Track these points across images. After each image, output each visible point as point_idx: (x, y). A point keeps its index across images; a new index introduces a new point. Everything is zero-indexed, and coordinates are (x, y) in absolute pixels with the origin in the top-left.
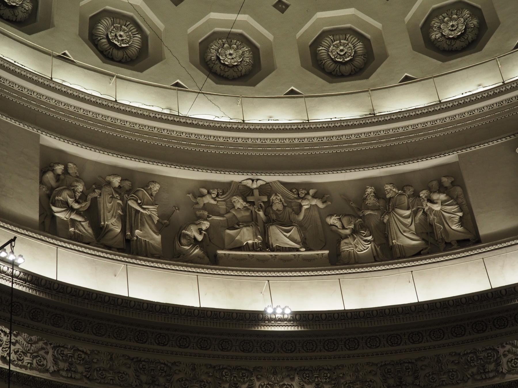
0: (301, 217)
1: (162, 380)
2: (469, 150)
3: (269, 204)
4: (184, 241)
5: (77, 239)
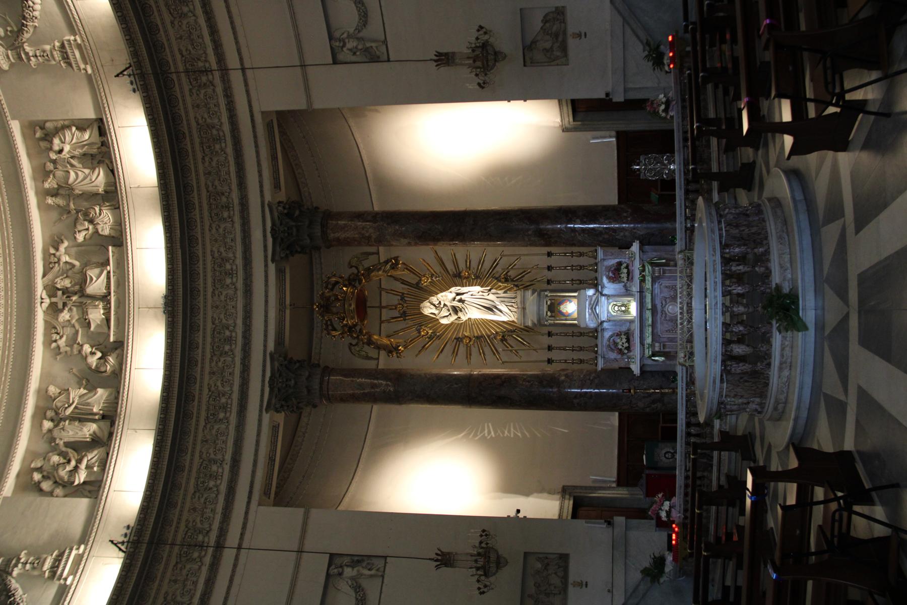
0: (77, 263)
1: (223, 400)
2: (6, 110)
3: (65, 291)
4: (103, 369)
5: (104, 464)
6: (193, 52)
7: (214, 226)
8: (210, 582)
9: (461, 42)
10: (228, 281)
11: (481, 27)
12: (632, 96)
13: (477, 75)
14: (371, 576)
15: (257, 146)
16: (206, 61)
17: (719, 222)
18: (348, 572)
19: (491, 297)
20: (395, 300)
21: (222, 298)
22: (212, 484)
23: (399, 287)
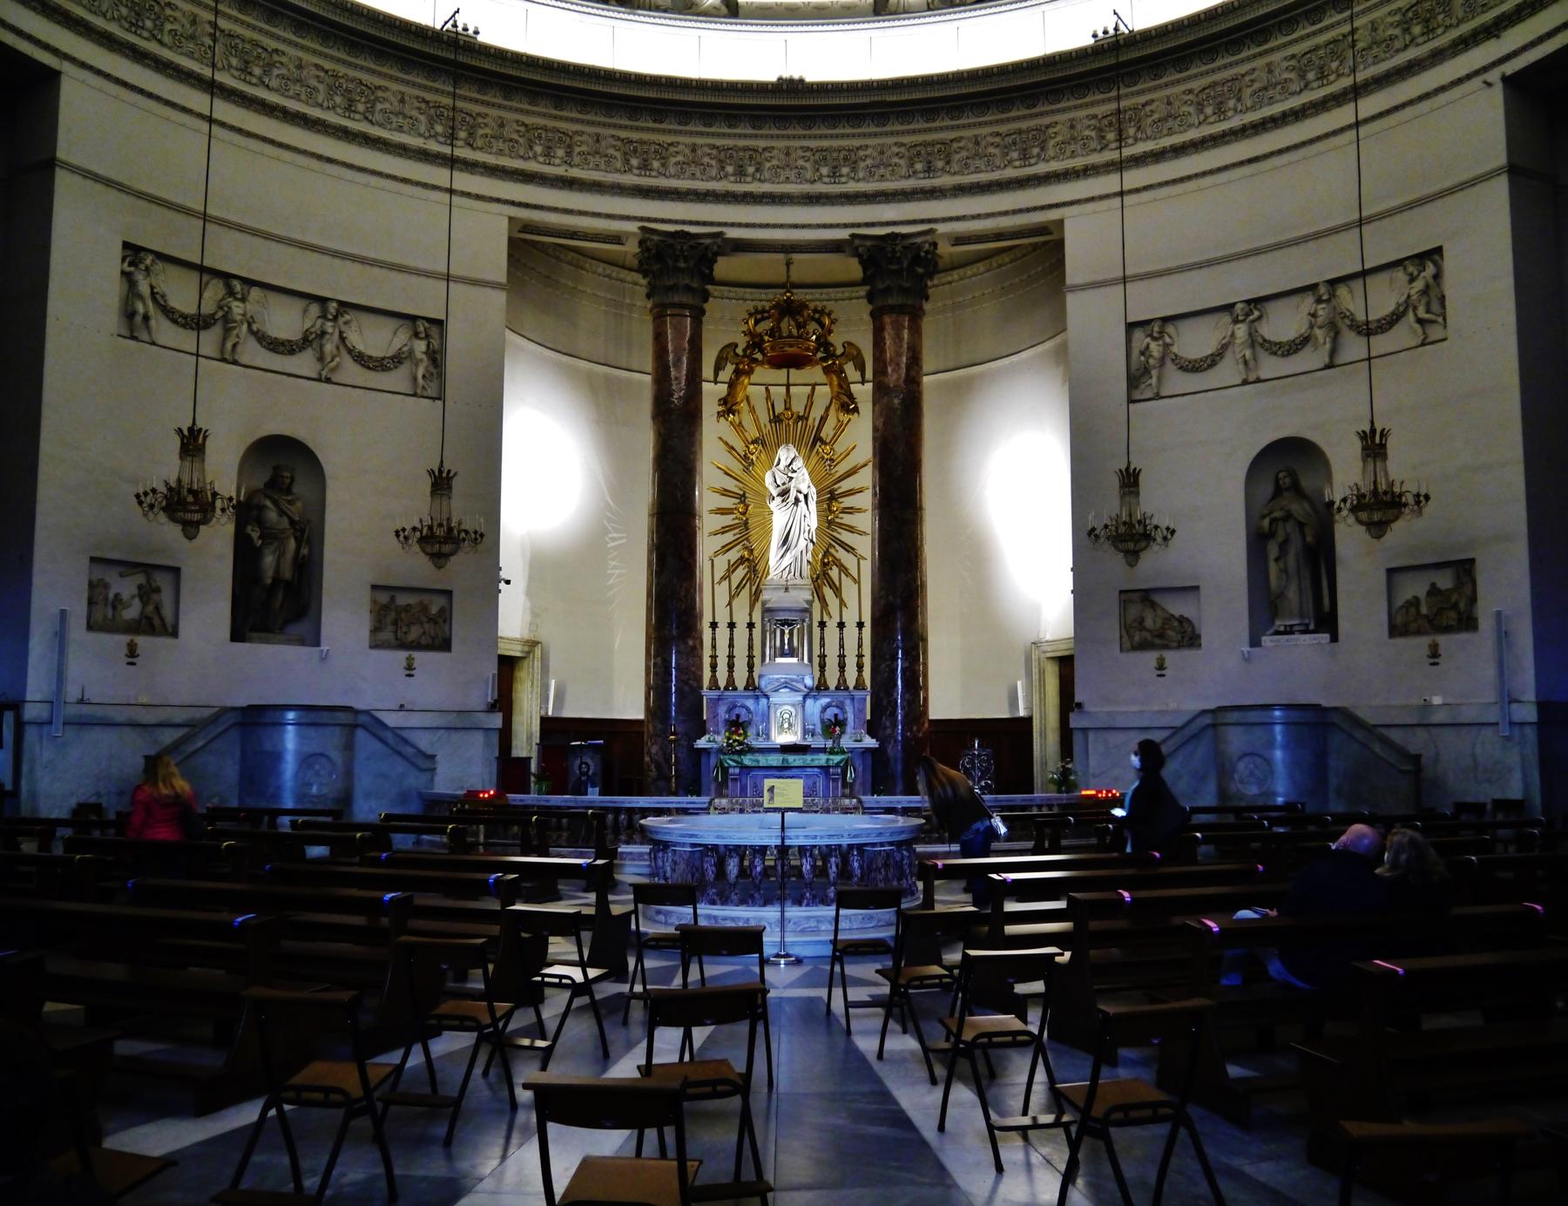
1: (656, 164)
6: (1149, 120)
7: (902, 150)
8: (403, 151)
9: (1154, 503)
10: (824, 171)
11: (1173, 532)
12: (1077, 739)
13: (1106, 526)
14: (415, 379)
15: (1015, 212)
16: (1136, 140)
17: (890, 844)
18: (420, 346)
19: (802, 543)
20: (798, 407)
21: (801, 163)
22: (538, 149)
23: (816, 413)
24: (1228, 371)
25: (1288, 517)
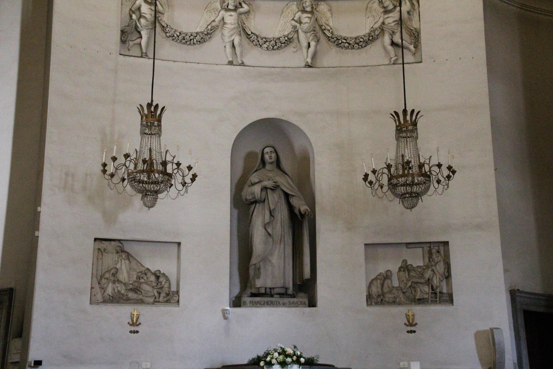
24: (217, 49)
25: (276, 188)
